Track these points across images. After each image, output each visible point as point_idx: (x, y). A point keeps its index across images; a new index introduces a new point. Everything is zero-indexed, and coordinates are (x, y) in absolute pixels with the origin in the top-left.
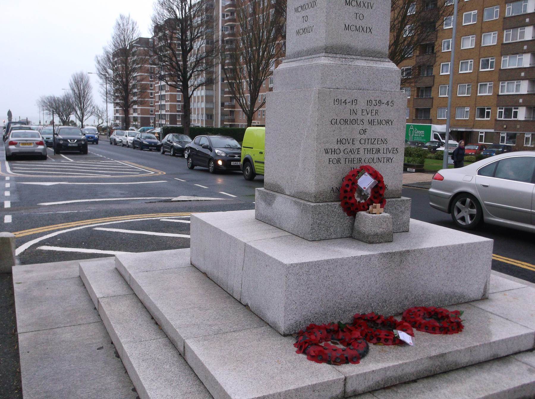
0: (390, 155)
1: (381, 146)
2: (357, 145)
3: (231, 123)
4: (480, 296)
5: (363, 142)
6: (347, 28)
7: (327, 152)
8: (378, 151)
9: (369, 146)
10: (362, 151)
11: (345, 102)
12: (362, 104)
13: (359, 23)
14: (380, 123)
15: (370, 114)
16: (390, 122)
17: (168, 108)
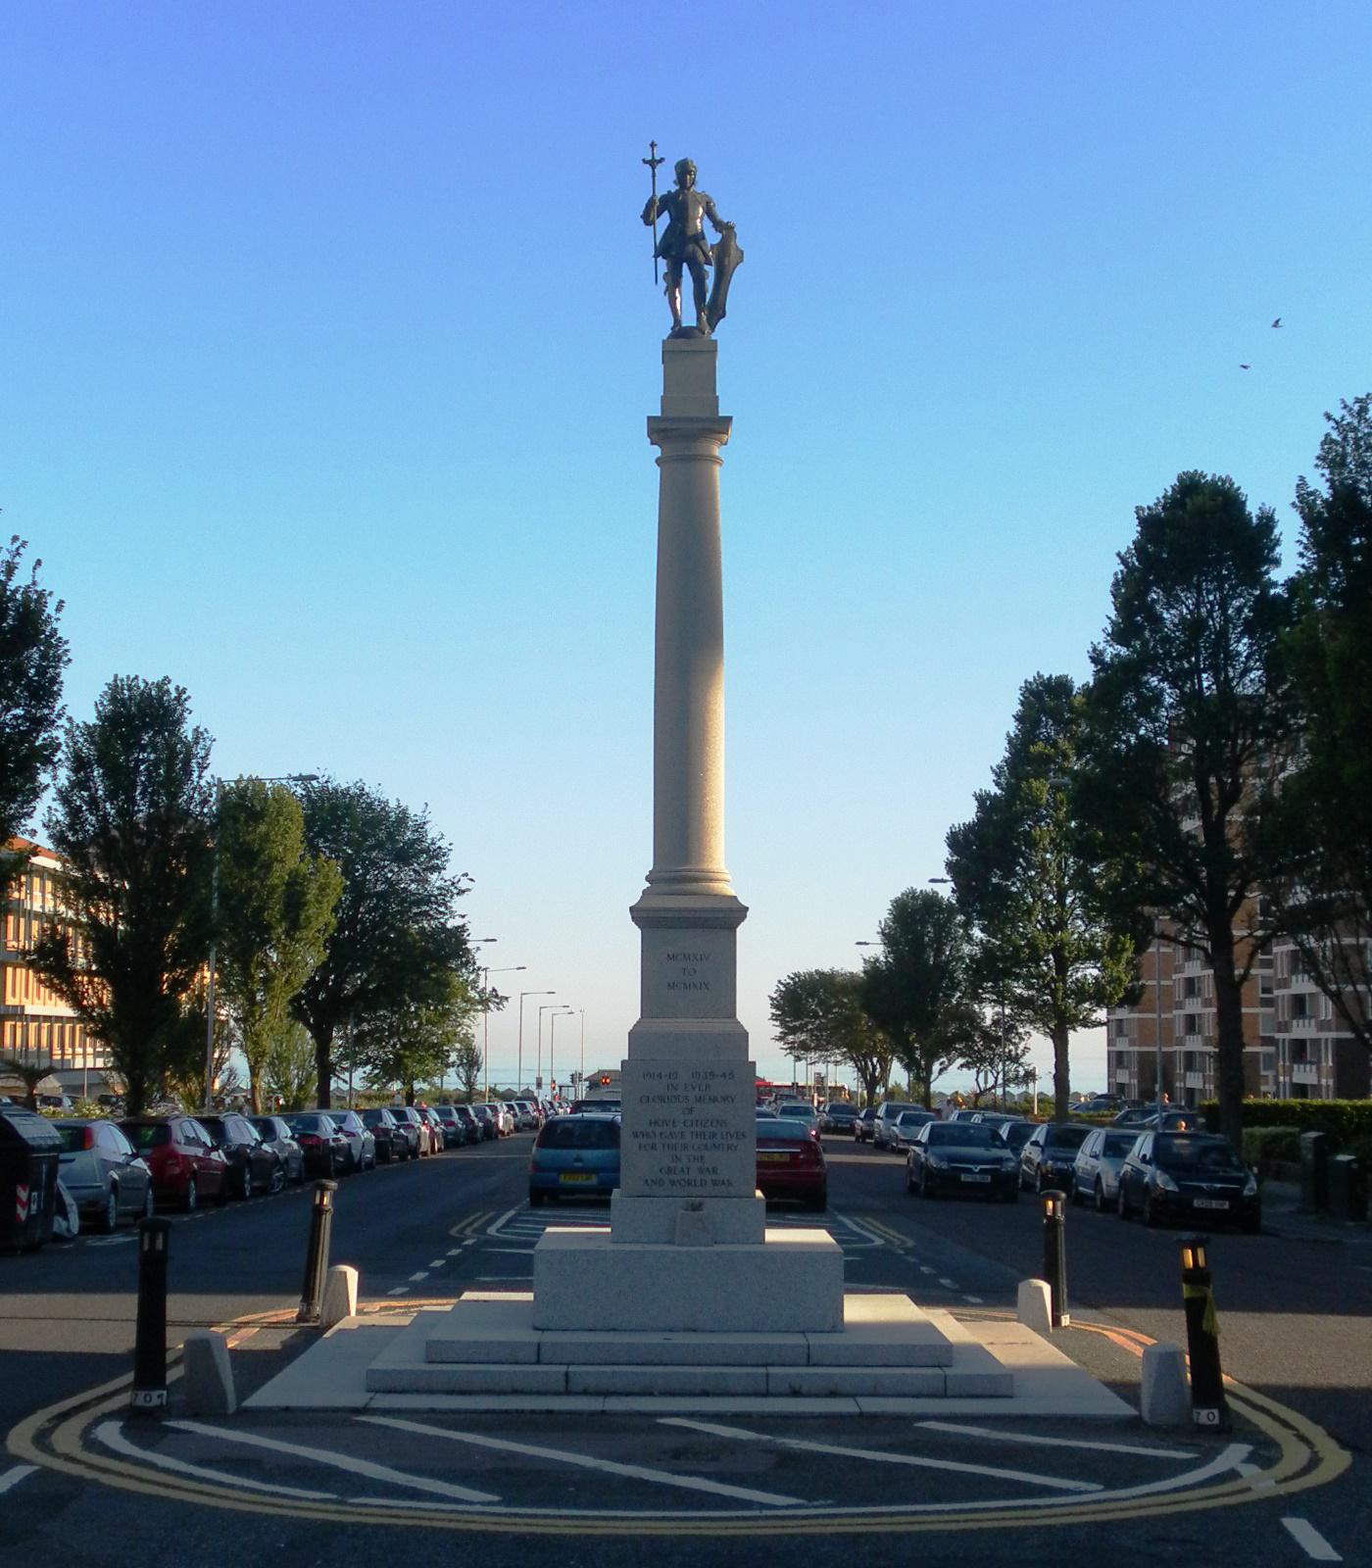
0: (734, 1141)
2: (680, 1127)
4: (827, 1327)
5: (689, 1123)
6: (672, 986)
7: (636, 1135)
8: (714, 1135)
9: (699, 1129)
10: (688, 1135)
11: (660, 1076)
14: (714, 1100)
15: (697, 1089)
16: (730, 1099)
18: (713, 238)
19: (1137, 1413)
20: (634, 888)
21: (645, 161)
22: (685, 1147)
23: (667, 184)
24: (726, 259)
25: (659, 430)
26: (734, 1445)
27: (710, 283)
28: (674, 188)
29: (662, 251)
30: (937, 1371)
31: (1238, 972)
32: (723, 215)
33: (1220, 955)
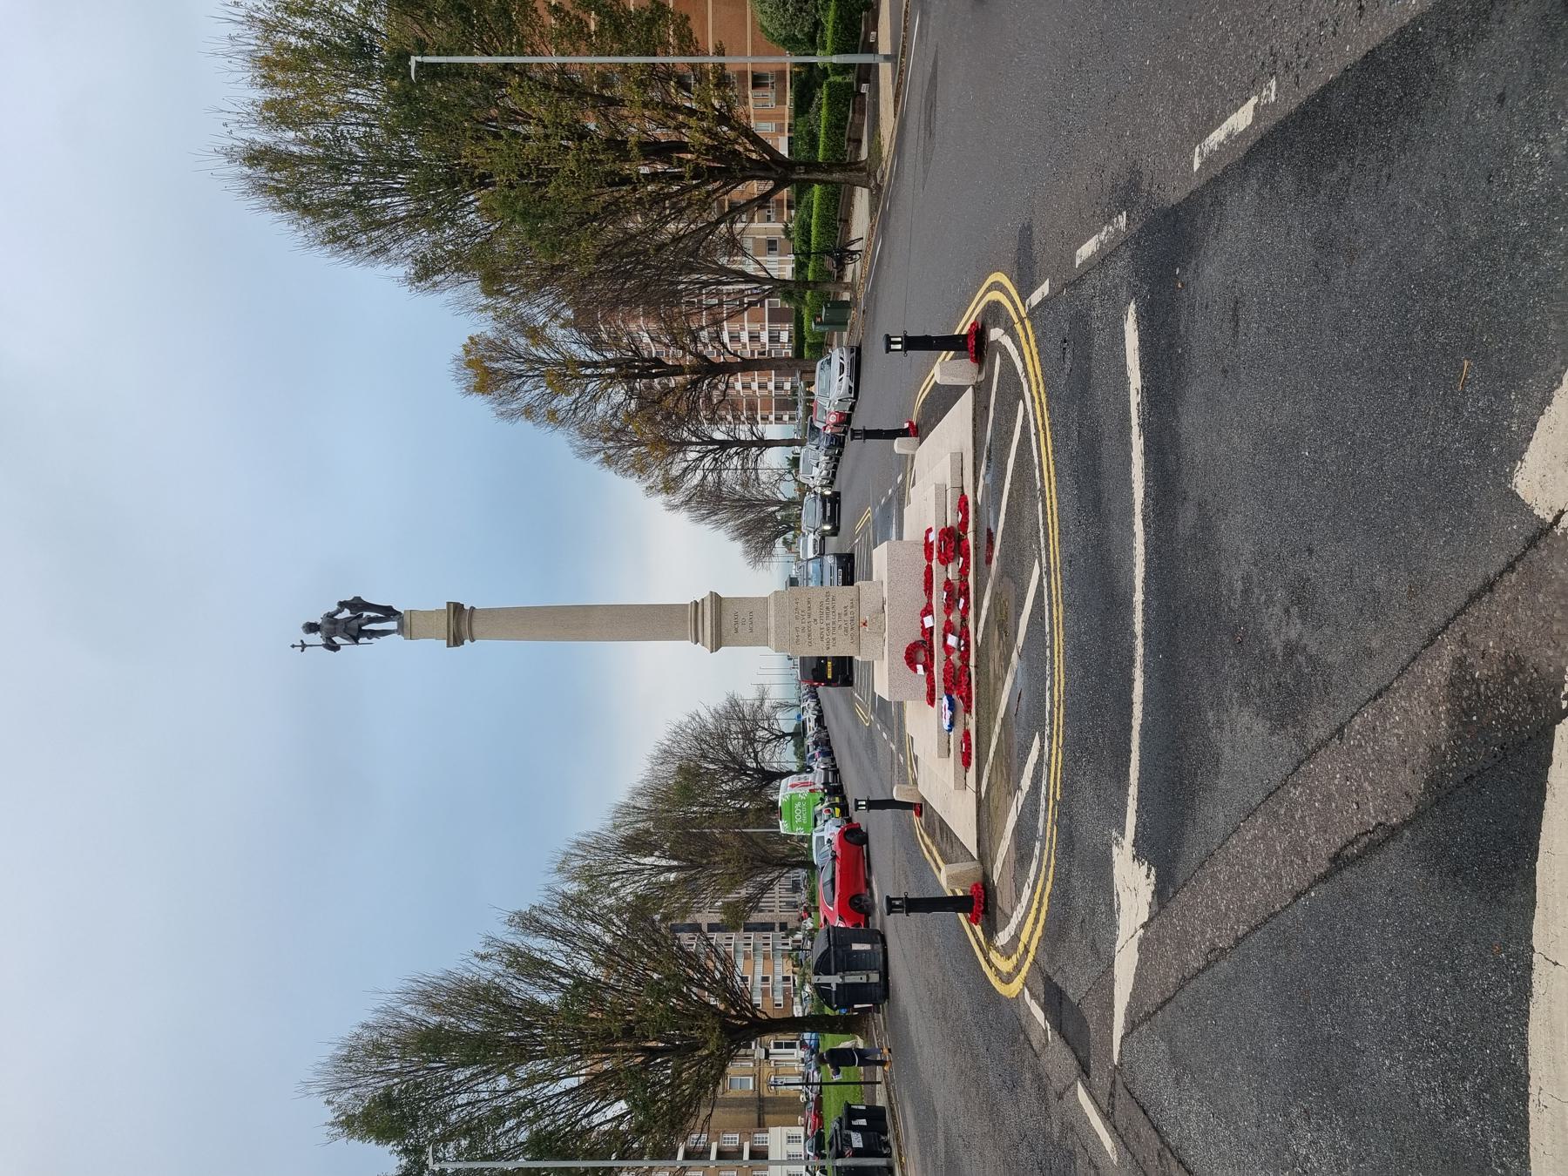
1: (825, 606)
2: (824, 626)
3: (785, 209)
10: (828, 622)
12: (798, 624)
13: (748, 622)
17: (757, 326)
18: (346, 613)
19: (970, 390)
20: (702, 650)
21: (302, 651)
22: (834, 623)
23: (317, 638)
24: (357, 605)
25: (456, 640)
26: (996, 597)
27: (373, 614)
28: (319, 634)
29: (356, 640)
30: (949, 492)
31: (739, 360)
32: (335, 607)
33: (728, 369)
